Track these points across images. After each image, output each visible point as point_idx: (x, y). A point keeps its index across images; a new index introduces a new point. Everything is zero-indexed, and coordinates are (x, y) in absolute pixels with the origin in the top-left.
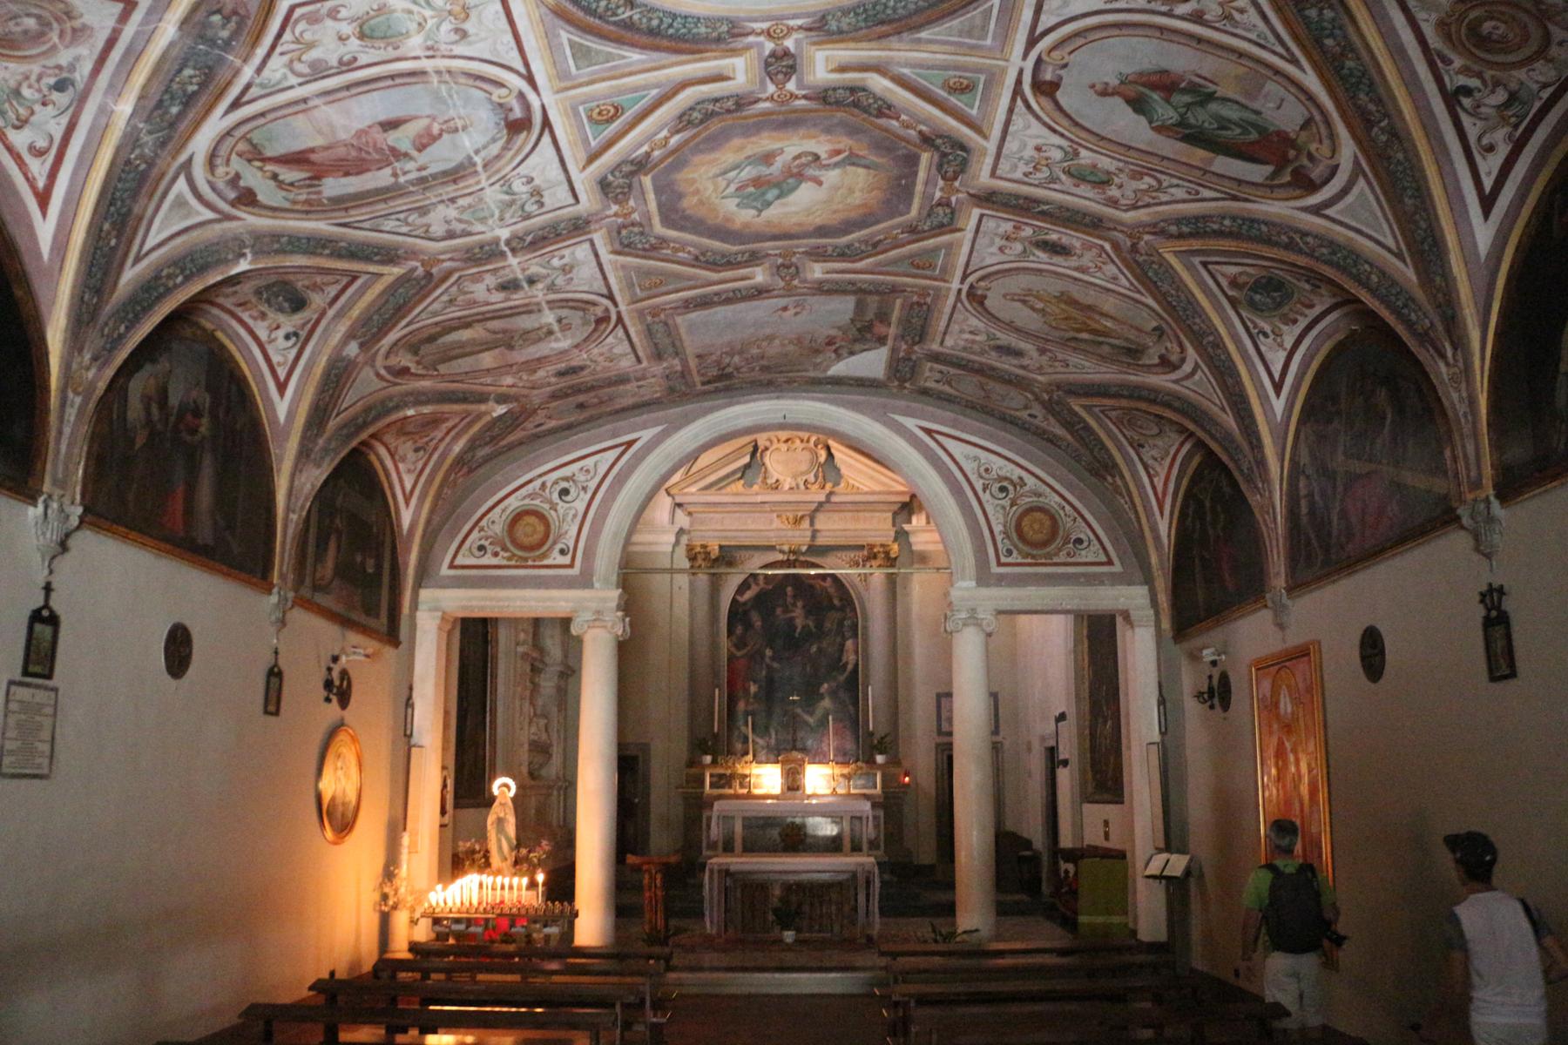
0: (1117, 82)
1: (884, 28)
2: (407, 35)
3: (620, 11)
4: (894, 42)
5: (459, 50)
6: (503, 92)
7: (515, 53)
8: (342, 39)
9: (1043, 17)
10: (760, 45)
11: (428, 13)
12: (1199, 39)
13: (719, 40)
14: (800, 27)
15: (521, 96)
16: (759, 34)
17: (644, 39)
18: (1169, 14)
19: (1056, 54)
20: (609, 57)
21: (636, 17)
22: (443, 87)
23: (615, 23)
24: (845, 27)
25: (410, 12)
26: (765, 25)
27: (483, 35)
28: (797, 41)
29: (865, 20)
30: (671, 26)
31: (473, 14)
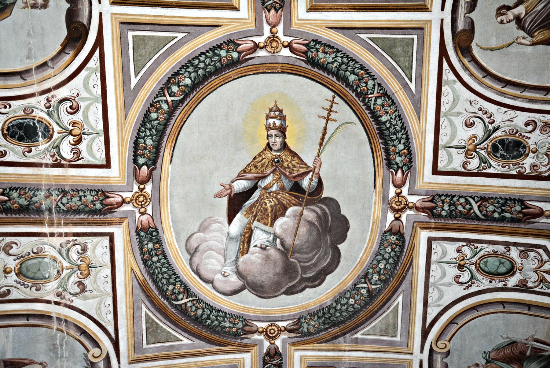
0: (484, 362)
1: (335, 330)
2: (47, 279)
3: (180, 296)
4: (341, 343)
5: (78, 303)
6: (97, 351)
7: (111, 317)
8: (6, 272)
9: (429, 310)
10: (261, 343)
11: (66, 264)
12: (529, 306)
13: (236, 335)
14: (286, 329)
15: (107, 359)
16: (261, 333)
17: (192, 326)
18: (505, 289)
19: (441, 344)
20: (169, 338)
21: (189, 304)
22: (59, 334)
23: (176, 307)
24: (312, 330)
25: (55, 260)
26: (264, 325)
27: (95, 293)
28: (283, 341)
29: (324, 323)
30: (208, 317)
31: (93, 272)
